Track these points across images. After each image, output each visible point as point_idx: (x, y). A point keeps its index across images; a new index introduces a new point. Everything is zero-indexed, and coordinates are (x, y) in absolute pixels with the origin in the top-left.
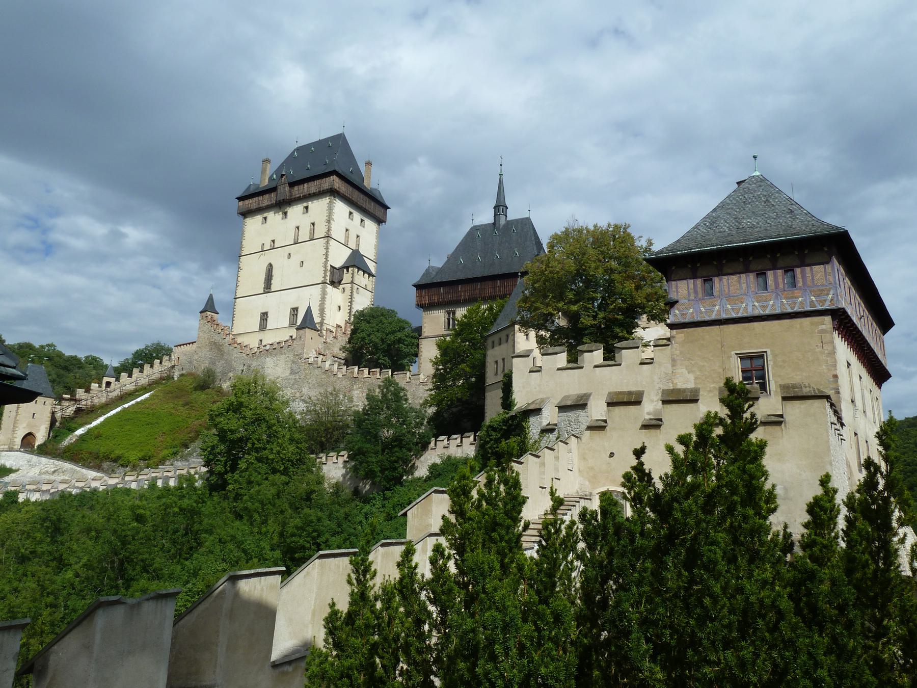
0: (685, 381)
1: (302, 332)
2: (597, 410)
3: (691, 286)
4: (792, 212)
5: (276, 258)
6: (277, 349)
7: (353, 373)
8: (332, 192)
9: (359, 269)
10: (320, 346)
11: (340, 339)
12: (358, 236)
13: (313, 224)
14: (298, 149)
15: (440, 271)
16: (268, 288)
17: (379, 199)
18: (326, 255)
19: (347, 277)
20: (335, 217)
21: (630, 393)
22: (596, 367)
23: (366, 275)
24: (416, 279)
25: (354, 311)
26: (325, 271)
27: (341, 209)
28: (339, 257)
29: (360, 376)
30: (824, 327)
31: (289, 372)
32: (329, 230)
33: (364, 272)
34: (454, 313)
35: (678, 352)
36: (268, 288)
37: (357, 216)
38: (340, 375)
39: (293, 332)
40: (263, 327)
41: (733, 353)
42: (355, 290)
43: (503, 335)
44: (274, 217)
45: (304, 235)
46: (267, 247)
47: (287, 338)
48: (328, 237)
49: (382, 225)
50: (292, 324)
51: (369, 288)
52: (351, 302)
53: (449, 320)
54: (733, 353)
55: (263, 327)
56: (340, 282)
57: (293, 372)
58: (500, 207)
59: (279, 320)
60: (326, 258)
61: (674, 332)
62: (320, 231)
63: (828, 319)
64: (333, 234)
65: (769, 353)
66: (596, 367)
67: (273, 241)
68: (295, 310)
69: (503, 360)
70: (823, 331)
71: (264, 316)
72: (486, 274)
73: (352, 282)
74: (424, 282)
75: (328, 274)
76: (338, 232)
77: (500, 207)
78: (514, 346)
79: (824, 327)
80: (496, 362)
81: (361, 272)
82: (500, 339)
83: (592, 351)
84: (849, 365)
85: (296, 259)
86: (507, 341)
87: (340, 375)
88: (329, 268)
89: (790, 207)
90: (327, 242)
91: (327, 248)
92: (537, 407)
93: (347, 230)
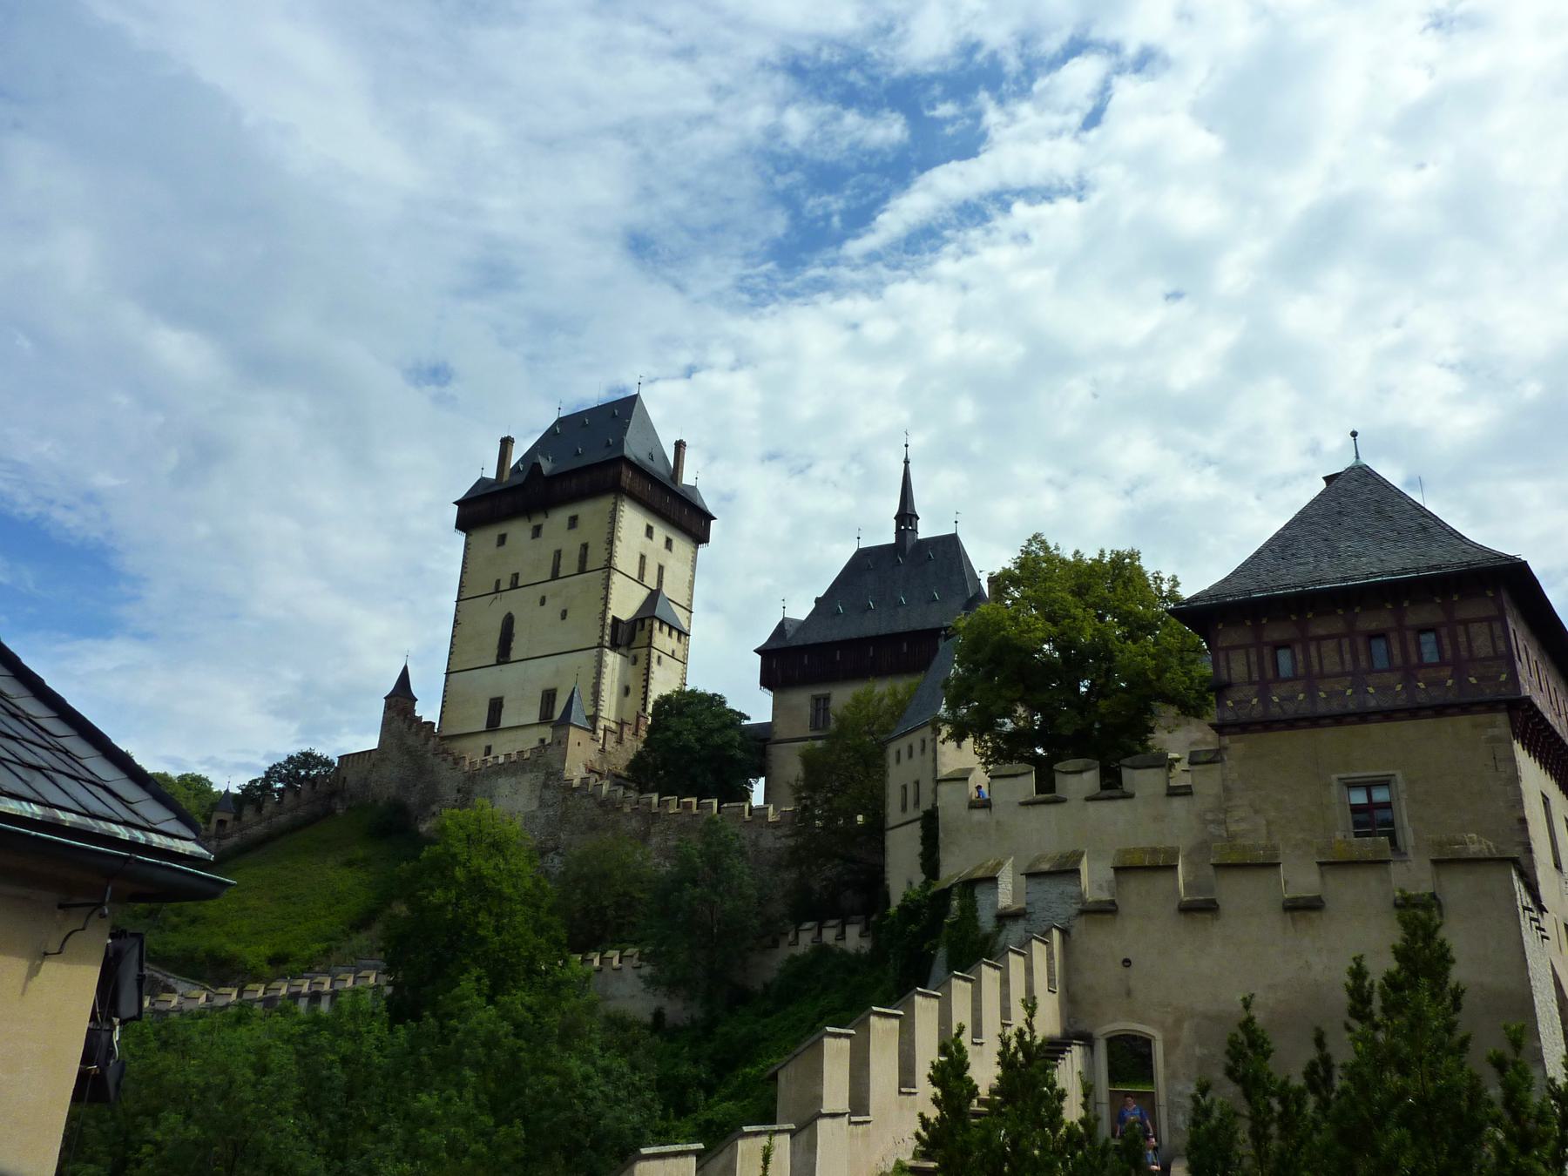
0: (1249, 828)
1: (561, 732)
2: (1093, 880)
3: (1253, 658)
4: (1425, 529)
5: (519, 603)
6: (515, 766)
7: (650, 804)
8: (618, 491)
9: (662, 622)
10: (593, 757)
11: (627, 743)
12: (661, 568)
13: (585, 547)
14: (560, 421)
15: (803, 626)
16: (504, 655)
17: (698, 503)
18: (606, 600)
19: (641, 637)
21: (1154, 851)
22: (1088, 799)
23: (675, 634)
24: (762, 639)
25: (654, 696)
27: (632, 520)
28: (625, 602)
29: (663, 811)
30: (1496, 731)
31: (535, 805)
33: (671, 628)
34: (827, 699)
35: (1235, 775)
36: (504, 655)
38: (627, 809)
39: (546, 733)
40: (493, 723)
41: (1334, 777)
42: (654, 660)
43: (915, 739)
44: (518, 531)
45: (569, 564)
46: (504, 585)
47: (536, 743)
49: (702, 549)
50: (546, 717)
51: (679, 655)
52: (647, 680)
53: (817, 710)
54: (1334, 777)
55: (493, 723)
56: (629, 645)
57: (543, 804)
58: (906, 516)
59: (522, 711)
60: (606, 604)
61: (1226, 740)
63: (1502, 718)
65: (1399, 777)
66: (1088, 799)
67: (516, 576)
68: (549, 697)
69: (917, 783)
70: (1494, 740)
71: (496, 706)
72: (883, 632)
73: (650, 645)
74: (774, 646)
75: (608, 631)
76: (625, 558)
77: (906, 516)
78: (935, 759)
79: (1496, 731)
80: (905, 787)
81: (666, 629)
82: (911, 747)
83: (1081, 772)
84: (1546, 800)
86: (923, 749)
87: (627, 809)
88: (609, 621)
89: (1420, 520)
90: (608, 578)
91: (607, 588)
92: (989, 874)
93: (643, 557)
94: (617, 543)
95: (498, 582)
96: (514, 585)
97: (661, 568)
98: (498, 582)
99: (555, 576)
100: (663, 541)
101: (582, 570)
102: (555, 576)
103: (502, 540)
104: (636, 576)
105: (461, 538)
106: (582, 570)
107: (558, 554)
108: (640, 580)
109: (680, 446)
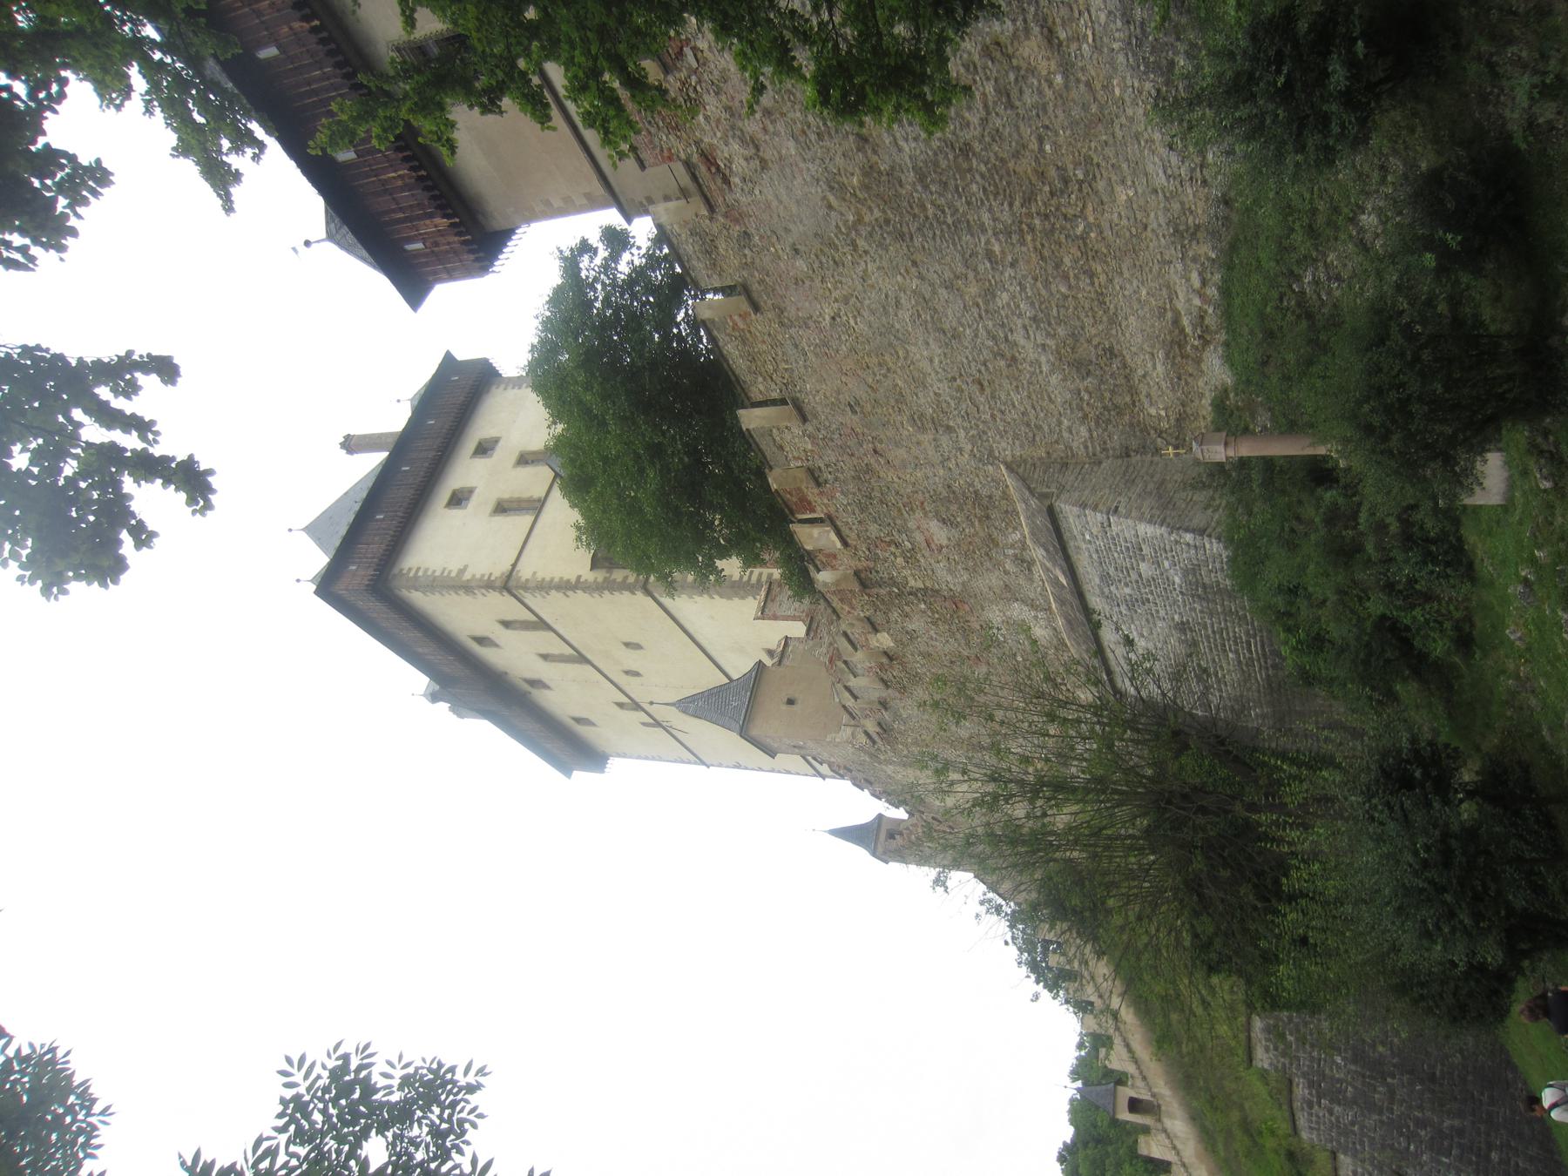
12: (524, 460)
18: (566, 587)
20: (454, 567)
25: (588, 575)
26: (609, 586)
32: (488, 585)
37: (465, 471)
38: (884, 640)
48: (508, 584)
62: (508, 607)
64: (499, 568)
75: (618, 575)
85: (632, 660)
87: (884, 640)
88: (600, 575)
90: (525, 588)
93: (501, 508)
94: (467, 576)
95: (644, 724)
96: (636, 706)
97: (524, 460)
98: (644, 724)
99: (581, 659)
100: (481, 464)
101: (541, 625)
102: (581, 659)
103: (578, 720)
104: (527, 520)
105: (614, 764)
106: (541, 625)
107: (545, 657)
108: (536, 507)
109: (352, 445)
